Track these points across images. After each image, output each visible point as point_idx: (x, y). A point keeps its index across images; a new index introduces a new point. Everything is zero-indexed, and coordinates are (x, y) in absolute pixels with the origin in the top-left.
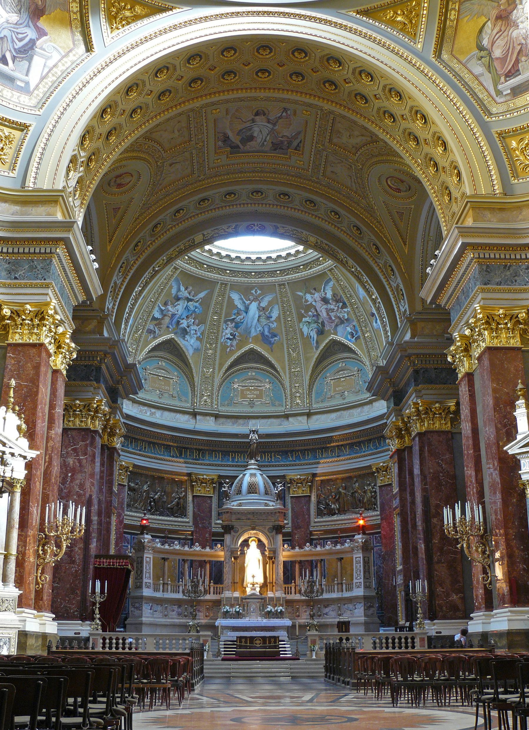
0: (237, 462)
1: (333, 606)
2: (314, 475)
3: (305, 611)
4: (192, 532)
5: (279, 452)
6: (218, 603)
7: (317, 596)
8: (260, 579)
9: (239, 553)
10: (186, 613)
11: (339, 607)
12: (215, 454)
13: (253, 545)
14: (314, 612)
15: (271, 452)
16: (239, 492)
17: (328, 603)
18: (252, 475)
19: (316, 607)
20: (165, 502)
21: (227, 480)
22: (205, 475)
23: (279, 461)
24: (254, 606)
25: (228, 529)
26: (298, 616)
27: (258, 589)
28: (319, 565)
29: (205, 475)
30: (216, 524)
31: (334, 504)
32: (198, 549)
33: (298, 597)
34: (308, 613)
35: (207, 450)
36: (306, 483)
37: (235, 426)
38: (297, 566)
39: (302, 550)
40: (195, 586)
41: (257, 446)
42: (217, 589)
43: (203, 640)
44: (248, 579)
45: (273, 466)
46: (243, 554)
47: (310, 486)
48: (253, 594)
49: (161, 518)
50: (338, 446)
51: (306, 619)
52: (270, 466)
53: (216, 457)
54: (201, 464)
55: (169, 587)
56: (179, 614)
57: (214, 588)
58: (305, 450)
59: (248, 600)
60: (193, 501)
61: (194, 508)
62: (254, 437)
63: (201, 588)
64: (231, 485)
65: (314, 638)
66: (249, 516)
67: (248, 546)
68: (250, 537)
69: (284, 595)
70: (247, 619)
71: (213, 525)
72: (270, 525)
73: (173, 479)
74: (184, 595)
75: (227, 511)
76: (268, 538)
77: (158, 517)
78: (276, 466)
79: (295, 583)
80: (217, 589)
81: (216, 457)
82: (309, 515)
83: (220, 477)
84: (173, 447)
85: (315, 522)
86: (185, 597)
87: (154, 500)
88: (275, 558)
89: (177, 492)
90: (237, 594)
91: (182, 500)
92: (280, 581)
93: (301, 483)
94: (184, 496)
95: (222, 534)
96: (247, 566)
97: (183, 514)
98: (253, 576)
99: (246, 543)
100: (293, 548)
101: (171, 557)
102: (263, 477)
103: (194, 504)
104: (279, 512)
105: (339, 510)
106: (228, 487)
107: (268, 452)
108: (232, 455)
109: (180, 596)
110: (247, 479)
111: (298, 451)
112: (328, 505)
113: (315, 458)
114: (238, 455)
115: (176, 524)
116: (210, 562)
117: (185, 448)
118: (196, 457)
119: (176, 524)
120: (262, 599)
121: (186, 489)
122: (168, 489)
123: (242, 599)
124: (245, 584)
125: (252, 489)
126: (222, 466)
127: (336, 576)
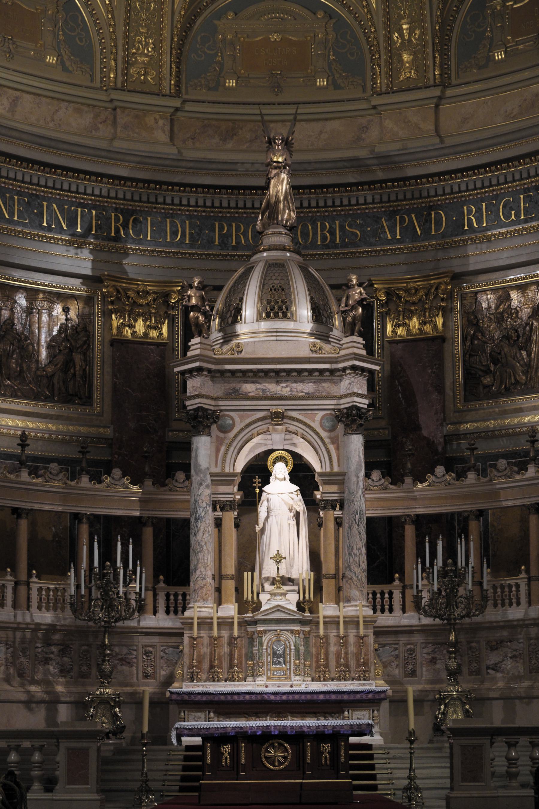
0: (235, 248)
7: (468, 615)
12: (173, 224)
37: (230, 145)
38: (410, 531)
42: (176, 600)
48: (279, 609)
53: (174, 233)
57: (168, 595)
59: (261, 628)
61: (114, 375)
68: (272, 451)
75: (197, 364)
79: (402, 579)
81: (174, 233)
88: (342, 508)
92: (357, 570)
96: (263, 530)
104: (354, 368)
108: (221, 228)
114: (238, 229)
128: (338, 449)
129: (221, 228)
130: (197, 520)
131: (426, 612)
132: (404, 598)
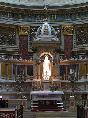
0: (39, 20)
1: (82, 85)
2: (74, 25)
3: (70, 88)
4: (19, 52)
5: (58, 15)
6: (31, 84)
8: (50, 74)
9: (40, 62)
10: (17, 89)
11: (85, 86)
13: (47, 58)
14: (74, 88)
15: (55, 15)
16: (40, 34)
17: (80, 84)
18: (45, 26)
19: (75, 86)
20: (6, 39)
21: (34, 29)
22: (24, 26)
23: (58, 19)
24: (46, 86)
25: (35, 51)
26: (67, 90)
27: (49, 78)
28: (76, 67)
29: (24, 26)
30: (30, 48)
31: (84, 38)
32: (22, 60)
33: (67, 81)
34: (71, 88)
35: (25, 14)
36: (71, 29)
37: (38, 2)
39: (69, 60)
40: (20, 77)
41: (48, 12)
42: (30, 78)
43: (23, 103)
44: (44, 74)
45: (56, 21)
46: (42, 62)
47: (73, 30)
48: (47, 80)
49: (4, 46)
50: (86, 12)
51: (71, 91)
52: (54, 21)
54: (22, 21)
55: (9, 77)
56: (13, 89)
57: (29, 77)
58: (71, 14)
59: (44, 83)
60: (19, 38)
61: (19, 41)
62: (46, 8)
63: (23, 78)
64: (36, 31)
65: (72, 101)
66: (44, 45)
67: (44, 58)
69: (60, 81)
70: (44, 91)
71: (28, 49)
72: (54, 49)
73: (10, 28)
74: (15, 81)
75: (34, 43)
76: (53, 55)
77: (3, 46)
78: (57, 21)
79: (65, 75)
80: (30, 78)
82: (72, 44)
83: (31, 26)
84: (9, 13)
85: (75, 47)
86: (16, 82)
87: (1, 38)
89: (12, 34)
90: (39, 80)
91: (14, 38)
93: (69, 29)
94: (15, 36)
95: (32, 53)
97: (15, 44)
98: (46, 72)
99: (43, 58)
100: (65, 59)
101: (9, 64)
102: (51, 27)
103: (19, 39)
104: (58, 43)
105: (86, 42)
106: (35, 32)
107: (53, 15)
108: (37, 16)
109: (14, 81)
110: (43, 28)
111: (67, 14)
112: (81, 39)
113: (75, 17)
115: (11, 48)
116: (27, 66)
117: (14, 13)
118: (20, 17)
119: (11, 48)
120: (50, 82)
121: (16, 32)
122: (7, 32)
123: (42, 82)
124: (43, 75)
125: (46, 32)
126: (32, 21)
127: (84, 72)
128: (55, 56)
129: (37, 16)
130: (34, 66)
131: (69, 80)
132: (66, 78)
